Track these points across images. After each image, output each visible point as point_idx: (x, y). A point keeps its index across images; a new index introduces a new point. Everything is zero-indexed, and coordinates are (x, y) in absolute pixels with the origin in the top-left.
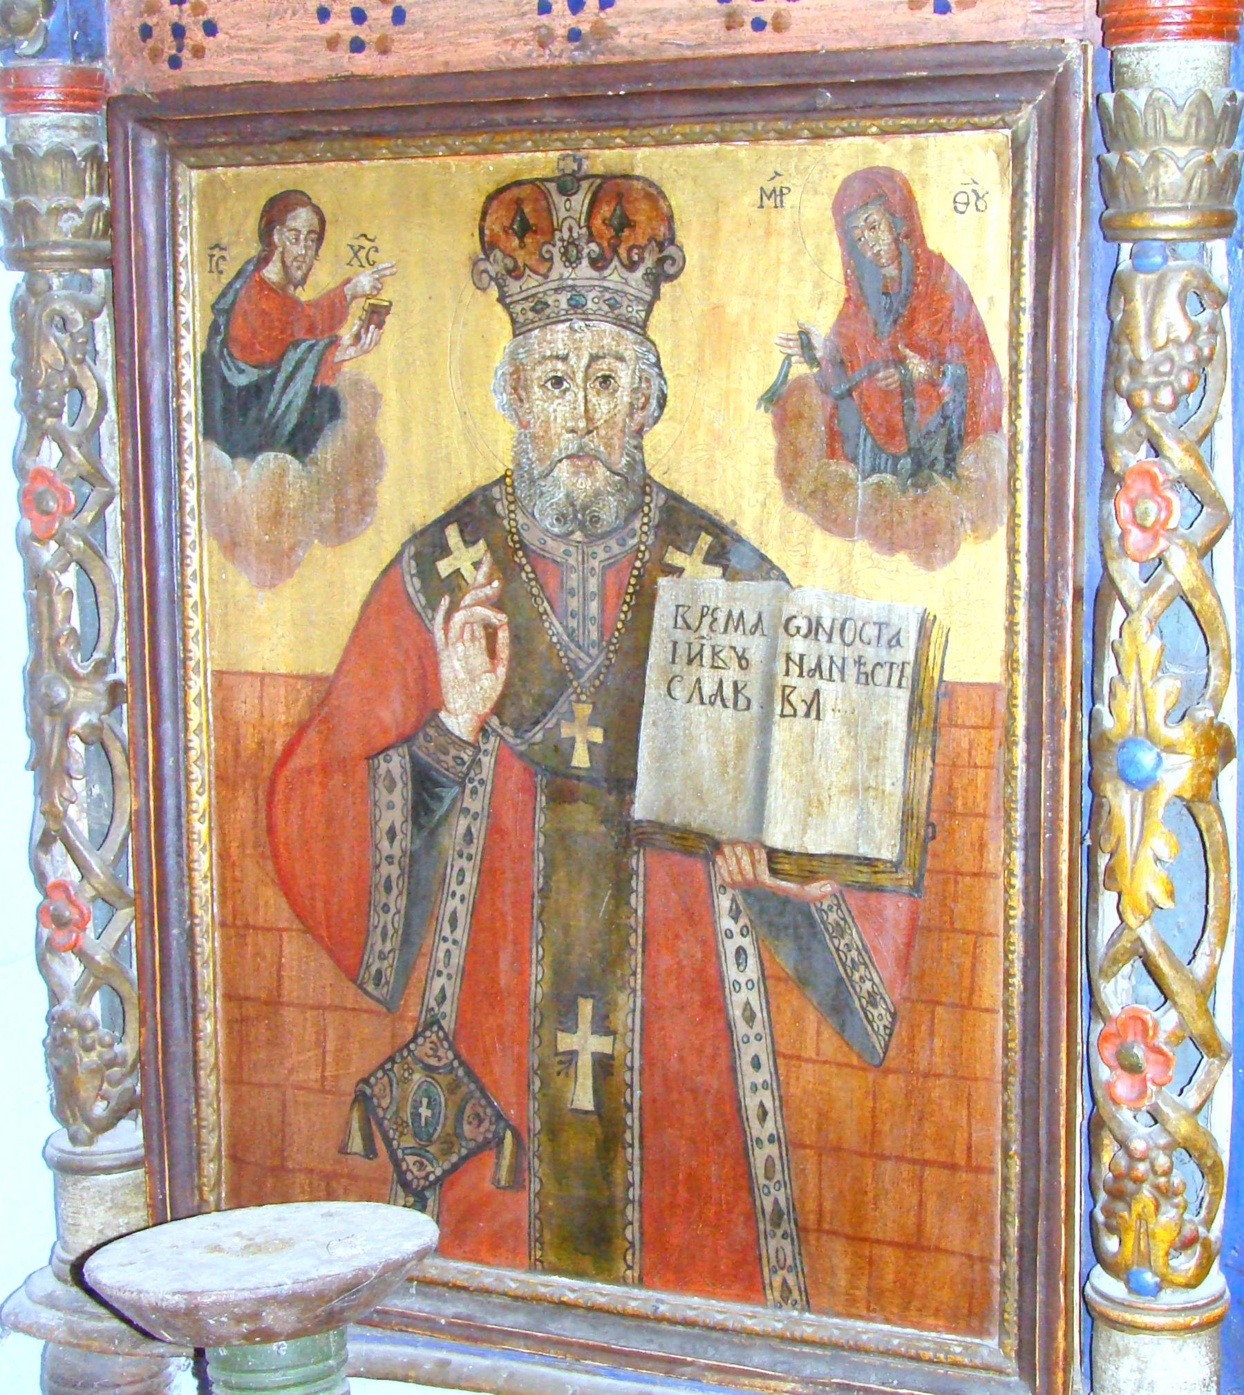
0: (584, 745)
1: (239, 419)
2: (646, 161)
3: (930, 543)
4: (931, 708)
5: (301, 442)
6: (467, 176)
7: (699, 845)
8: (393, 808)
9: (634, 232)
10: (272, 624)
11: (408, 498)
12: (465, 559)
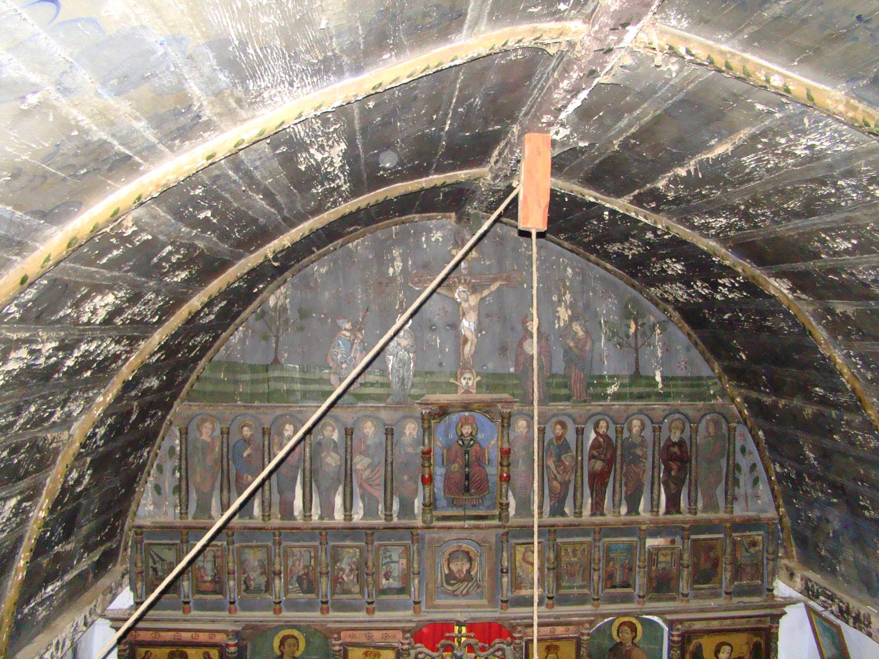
2: (185, 650)
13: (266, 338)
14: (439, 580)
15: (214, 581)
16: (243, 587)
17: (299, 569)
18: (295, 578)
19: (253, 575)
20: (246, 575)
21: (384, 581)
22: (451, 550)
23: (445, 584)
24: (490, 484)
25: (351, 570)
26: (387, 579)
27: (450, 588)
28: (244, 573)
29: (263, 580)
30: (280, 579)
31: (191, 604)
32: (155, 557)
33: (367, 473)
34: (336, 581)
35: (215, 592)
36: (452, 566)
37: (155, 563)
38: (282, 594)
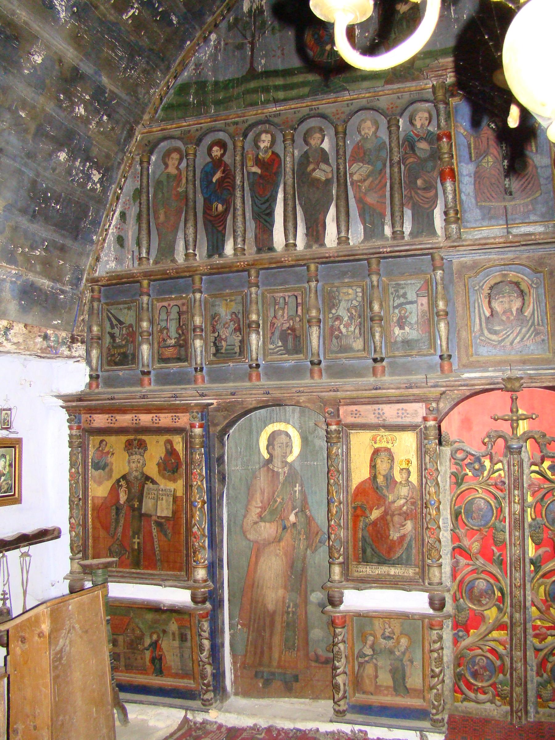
0: (136, 504)
1: (97, 466)
2: (144, 437)
3: (175, 480)
4: (175, 499)
5: (103, 469)
6: (124, 439)
7: (148, 516)
8: (114, 513)
9: (142, 445)
10: (99, 490)
11: (116, 476)
12: (123, 483)
13: (240, 47)
14: (477, 327)
15: (178, 345)
16: (213, 350)
17: (283, 321)
18: (277, 334)
19: (225, 333)
20: (216, 335)
21: (397, 331)
22: (492, 282)
23: (486, 332)
24: (542, 181)
25: (351, 318)
26: (402, 327)
27: (494, 337)
28: (214, 332)
29: (236, 339)
30: (258, 333)
31: (152, 376)
32: (113, 319)
33: (367, 183)
34: (332, 334)
35: (179, 360)
36: (496, 305)
37: (112, 327)
38: (261, 357)
